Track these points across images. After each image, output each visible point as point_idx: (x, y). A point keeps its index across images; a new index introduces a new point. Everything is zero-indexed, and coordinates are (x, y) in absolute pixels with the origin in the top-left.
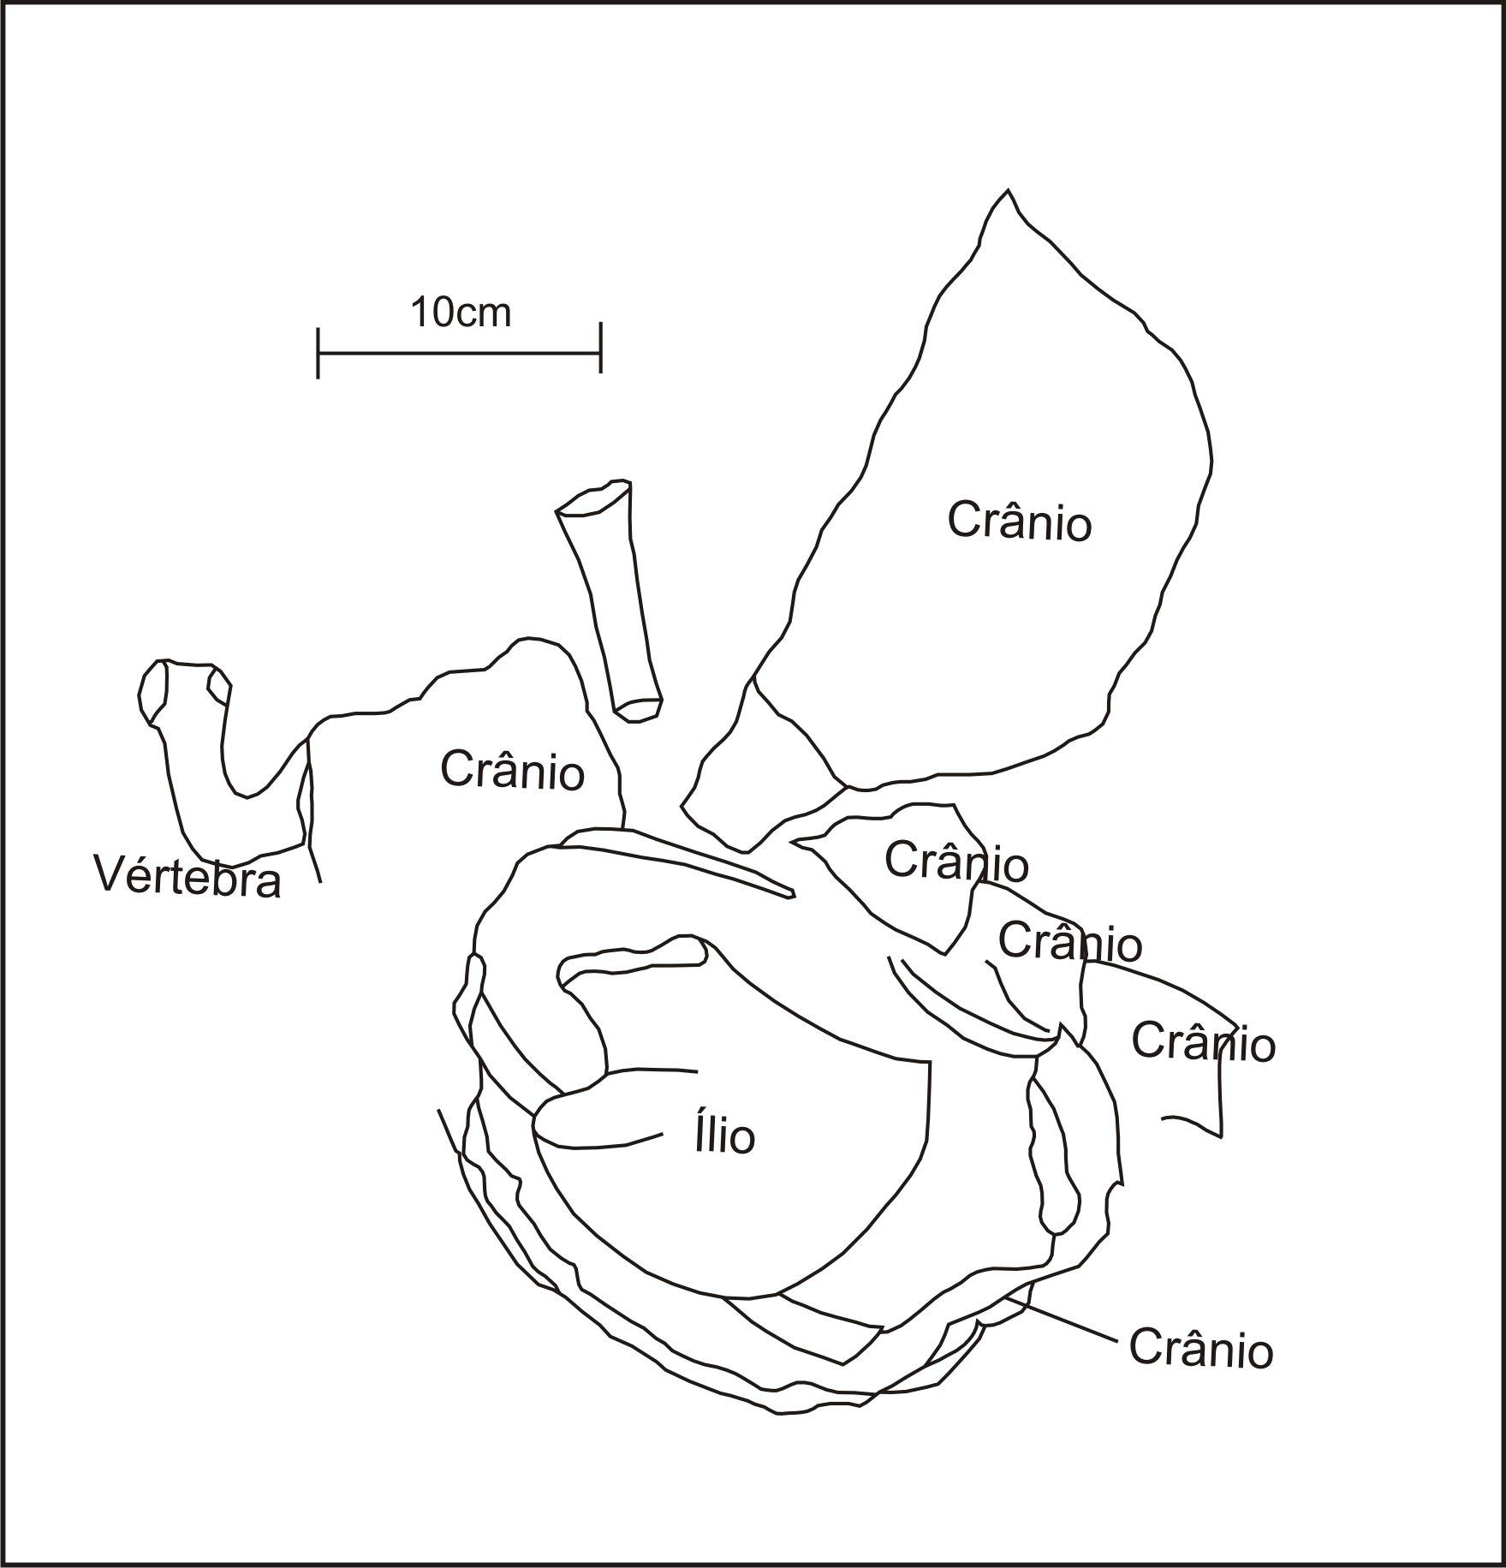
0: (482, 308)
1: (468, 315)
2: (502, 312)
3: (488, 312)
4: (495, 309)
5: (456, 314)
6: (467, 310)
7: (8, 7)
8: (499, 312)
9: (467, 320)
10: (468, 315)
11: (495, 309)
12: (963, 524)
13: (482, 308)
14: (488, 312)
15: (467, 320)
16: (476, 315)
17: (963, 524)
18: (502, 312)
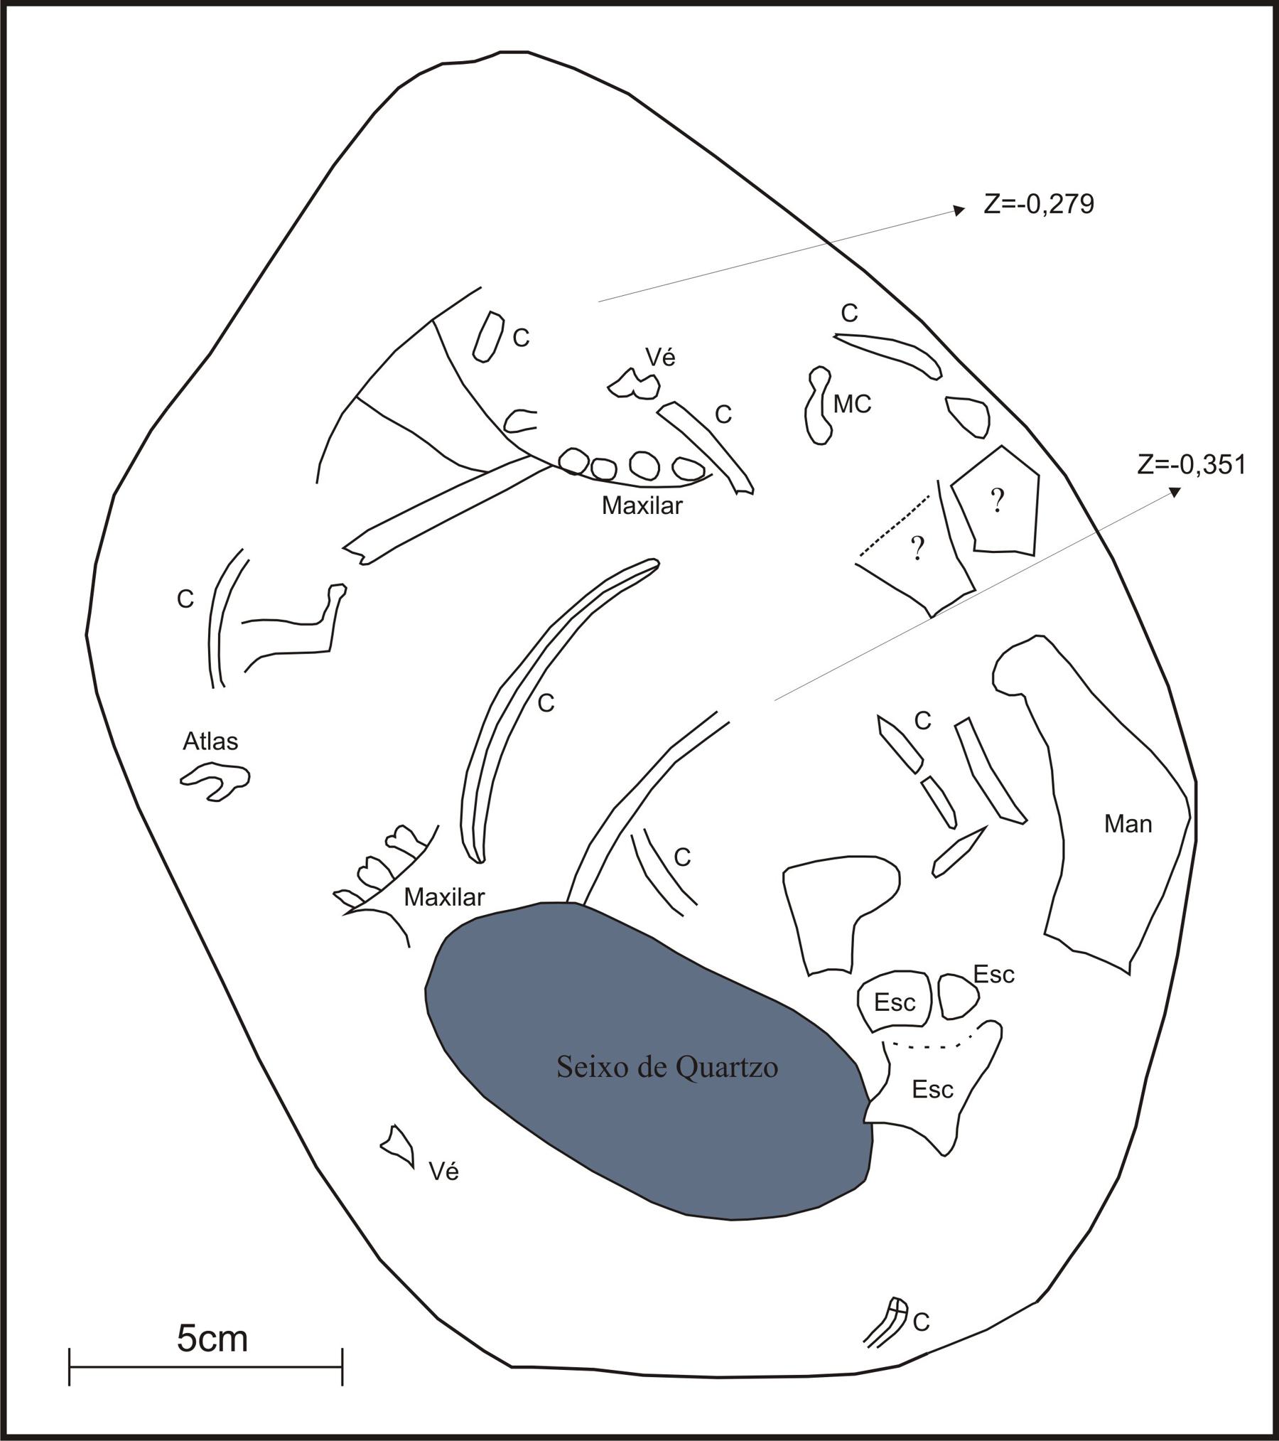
0: (222, 1335)
1: (209, 1341)
2: (239, 1338)
3: (227, 1338)
4: (233, 1336)
5: (197, 1342)
6: (208, 1336)
7: (10, 9)
8: (237, 1338)
9: (208, 1345)
11: (233, 1336)
13: (222, 1335)
14: (227, 1338)
15: (208, 1345)
16: (217, 1341)
18: (239, 1338)
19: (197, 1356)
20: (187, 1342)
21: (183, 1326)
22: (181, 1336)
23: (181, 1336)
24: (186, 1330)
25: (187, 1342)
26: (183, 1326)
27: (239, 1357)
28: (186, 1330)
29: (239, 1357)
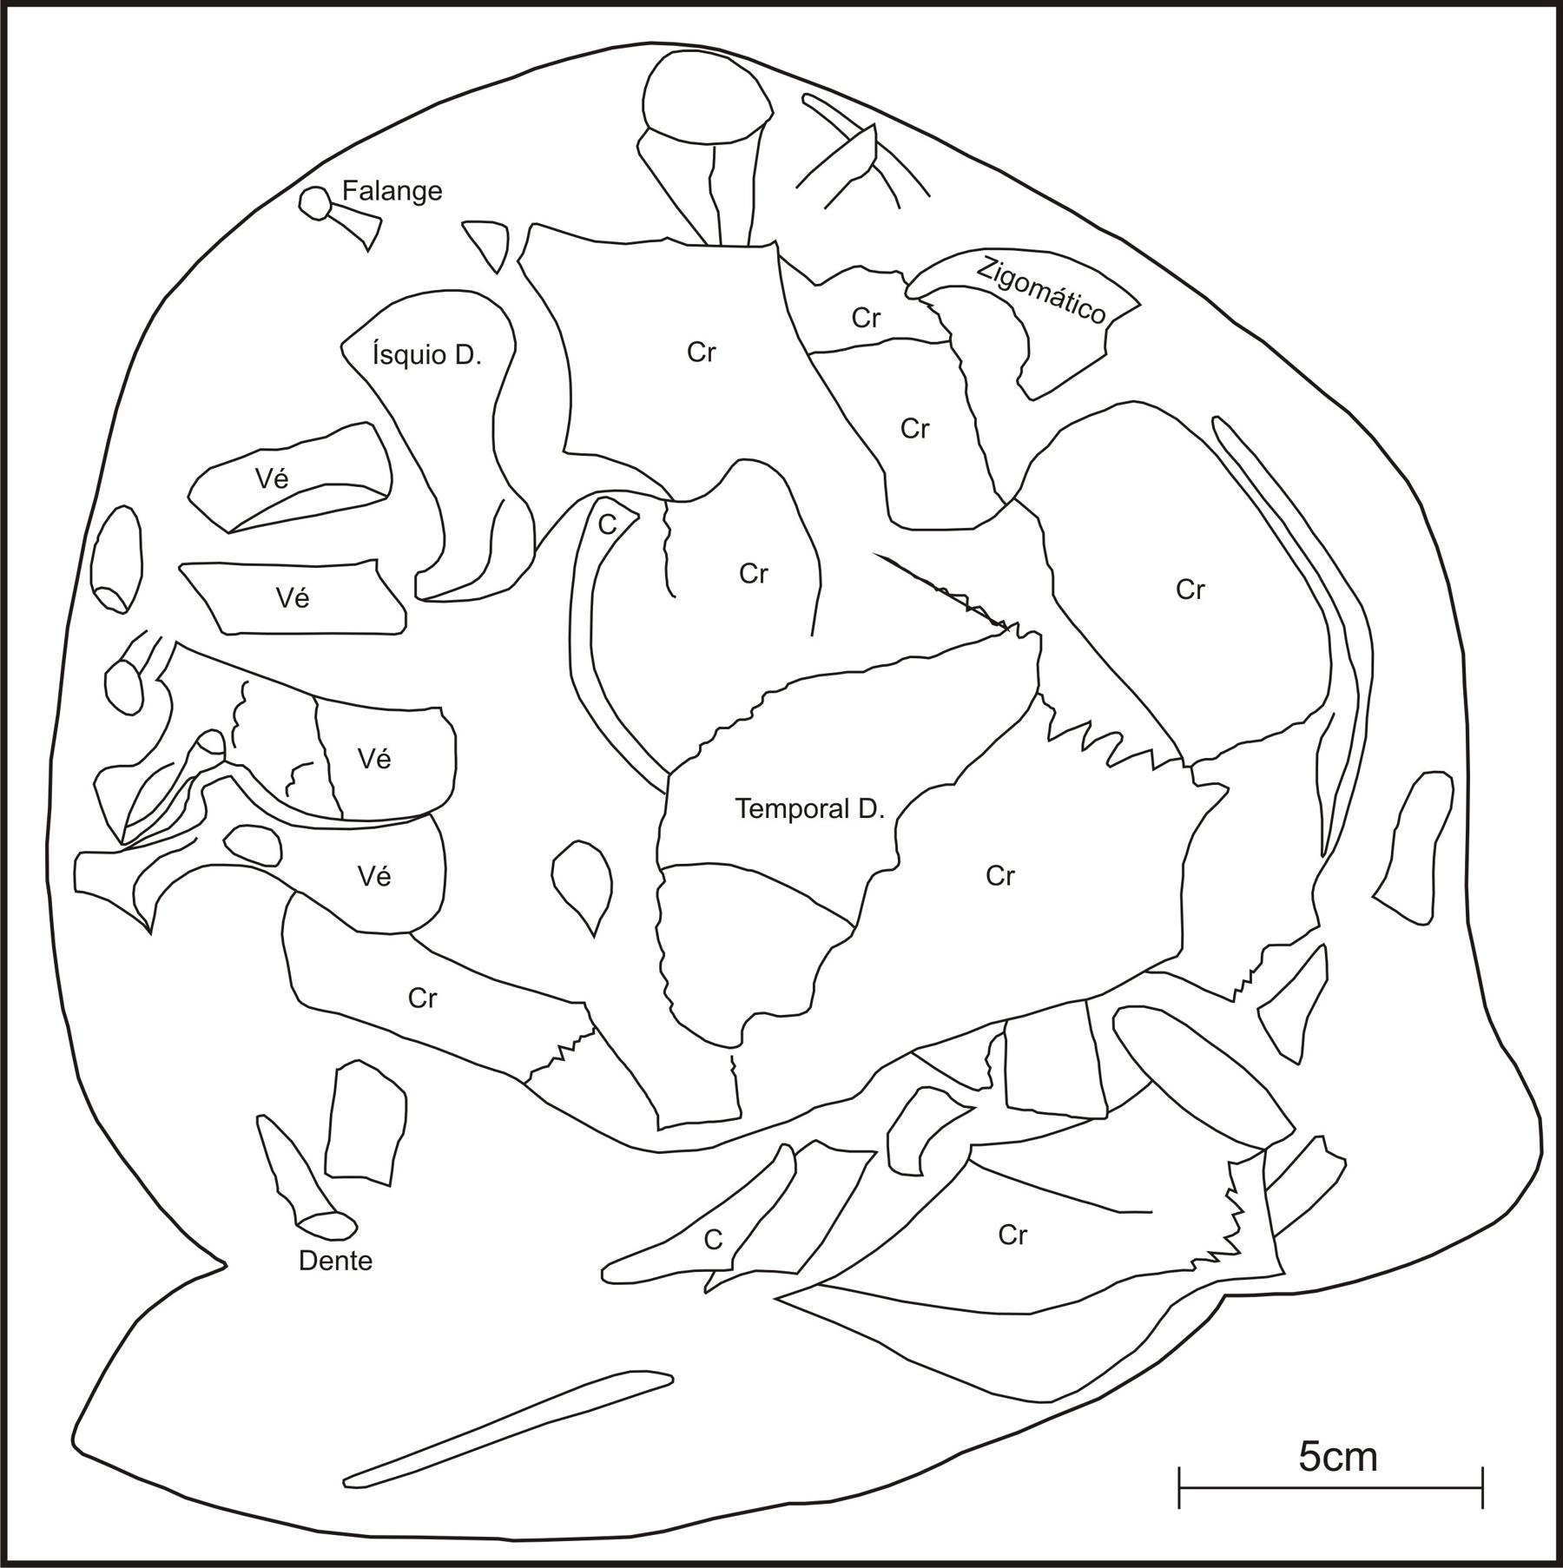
0: (1349, 1452)
1: (1334, 1460)
2: (1368, 1457)
3: (1355, 1457)
4: (1361, 1454)
5: (1322, 1461)
6: (1333, 1455)
8: (1365, 1455)
10: (1334, 1460)
11: (1361, 1454)
12: (1084, 312)
13: (1349, 1452)
14: (1355, 1457)
16: (1343, 1459)
17: (1084, 312)
18: (1368, 1457)
19: (1322, 1476)
20: (1310, 1461)
21: (1306, 1443)
22: (1303, 1454)
23: (1303, 1454)
24: (1309, 1447)
25: (1310, 1461)
26: (1306, 1443)
27: (1368, 1477)
28: (1309, 1447)
29: (1368, 1477)
